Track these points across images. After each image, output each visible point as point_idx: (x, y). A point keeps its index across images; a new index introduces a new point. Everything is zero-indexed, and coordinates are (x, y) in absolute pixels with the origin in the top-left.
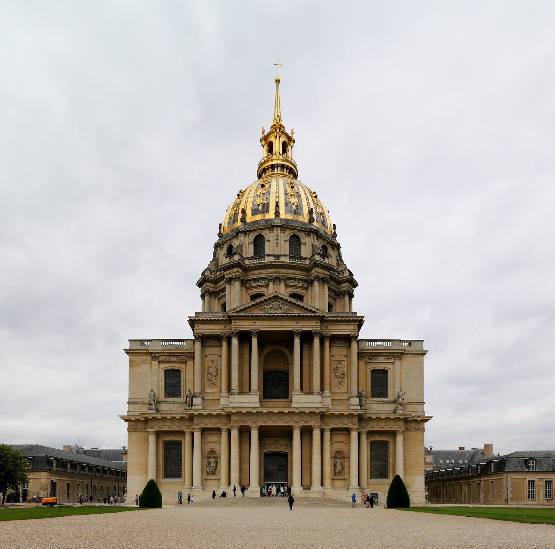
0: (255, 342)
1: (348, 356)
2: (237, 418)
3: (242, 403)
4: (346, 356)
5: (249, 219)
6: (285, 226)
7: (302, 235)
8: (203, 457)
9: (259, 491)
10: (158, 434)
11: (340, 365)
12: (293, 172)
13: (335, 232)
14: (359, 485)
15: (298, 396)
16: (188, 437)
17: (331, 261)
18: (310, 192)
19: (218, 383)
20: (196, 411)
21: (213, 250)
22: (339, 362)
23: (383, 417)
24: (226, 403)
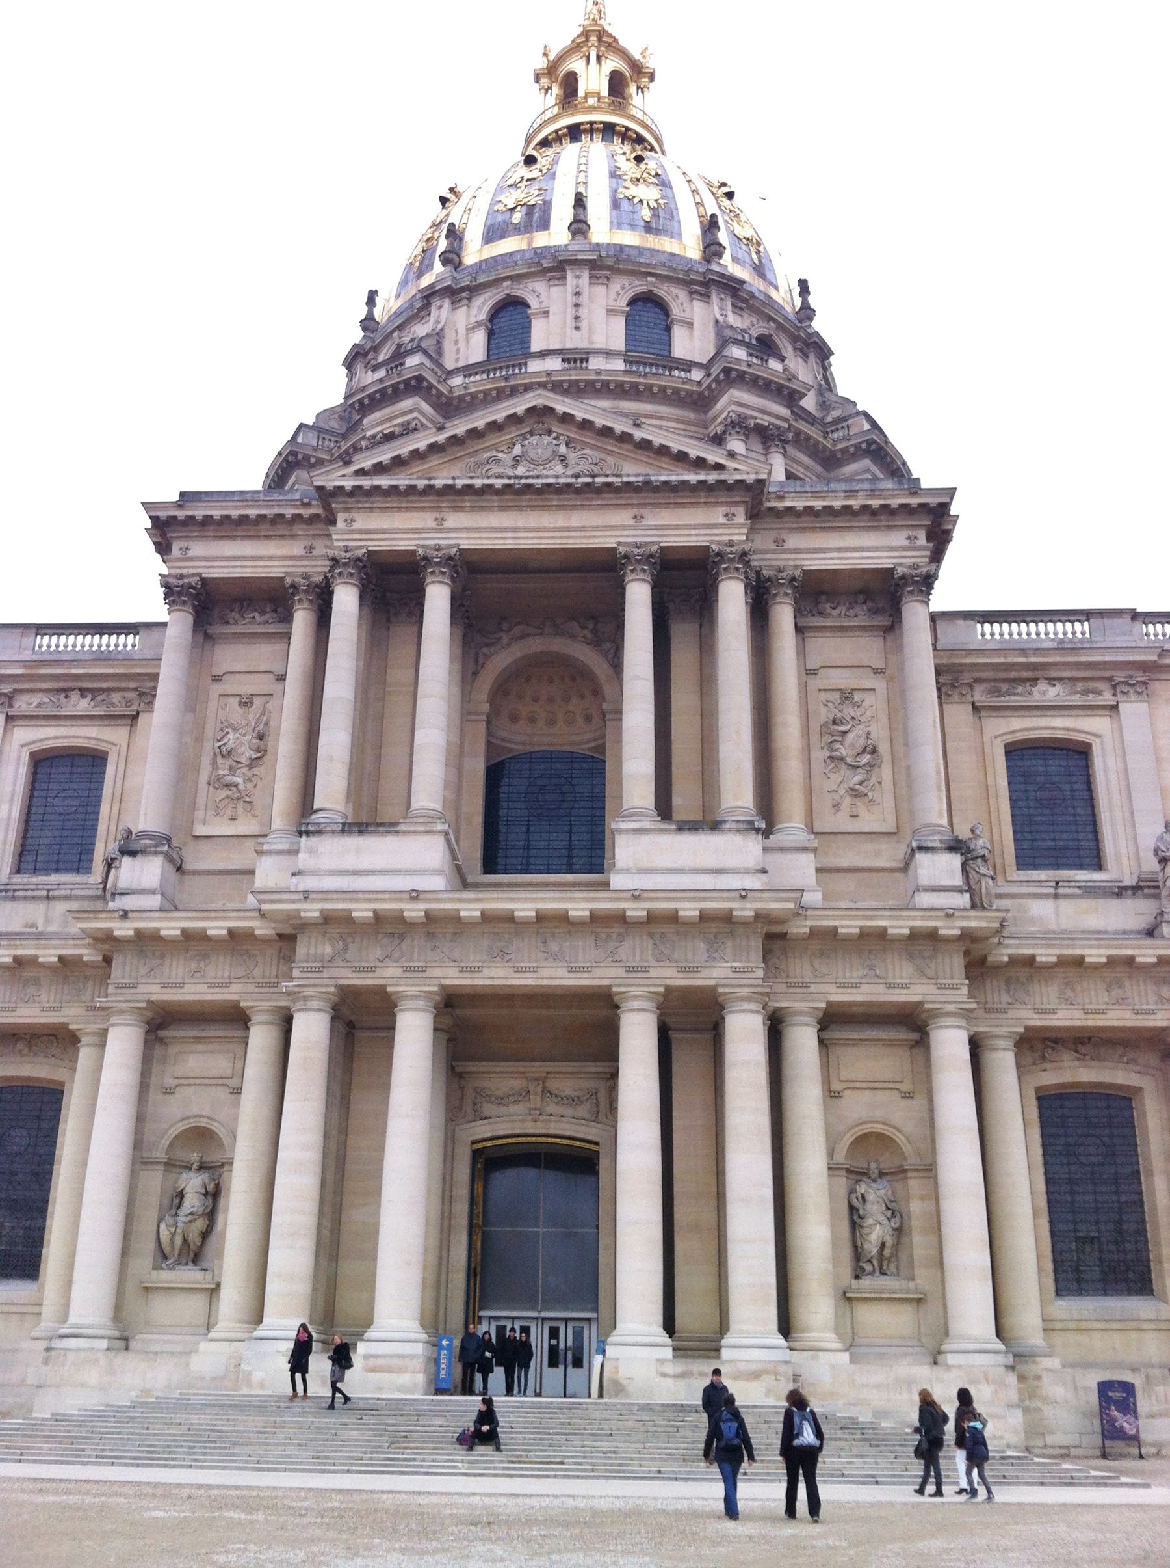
1: (892, 672)
2: (328, 950)
3: (356, 873)
7: (679, 301)
9: (419, 1364)
14: (999, 1333)
15: (646, 839)
18: (709, 185)
20: (125, 915)
23: (1095, 954)
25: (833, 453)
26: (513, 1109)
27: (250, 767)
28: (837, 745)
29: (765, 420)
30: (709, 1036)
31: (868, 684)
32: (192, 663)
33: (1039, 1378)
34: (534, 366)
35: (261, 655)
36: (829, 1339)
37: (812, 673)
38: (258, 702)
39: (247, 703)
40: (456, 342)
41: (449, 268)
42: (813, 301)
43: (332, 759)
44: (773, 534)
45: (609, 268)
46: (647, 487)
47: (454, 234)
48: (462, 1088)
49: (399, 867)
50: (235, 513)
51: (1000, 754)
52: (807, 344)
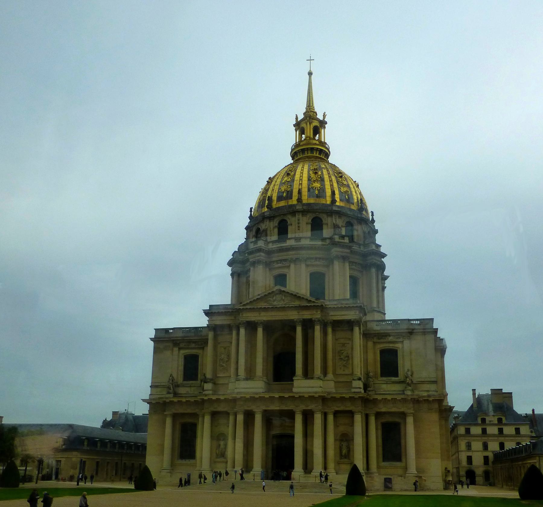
5: (275, 205)
6: (308, 209)
7: (324, 217)
15: (299, 381)
23: (389, 397)
29: (344, 254)
31: (348, 342)
36: (333, 471)
37: (336, 340)
46: (300, 306)
47: (270, 199)
51: (378, 352)
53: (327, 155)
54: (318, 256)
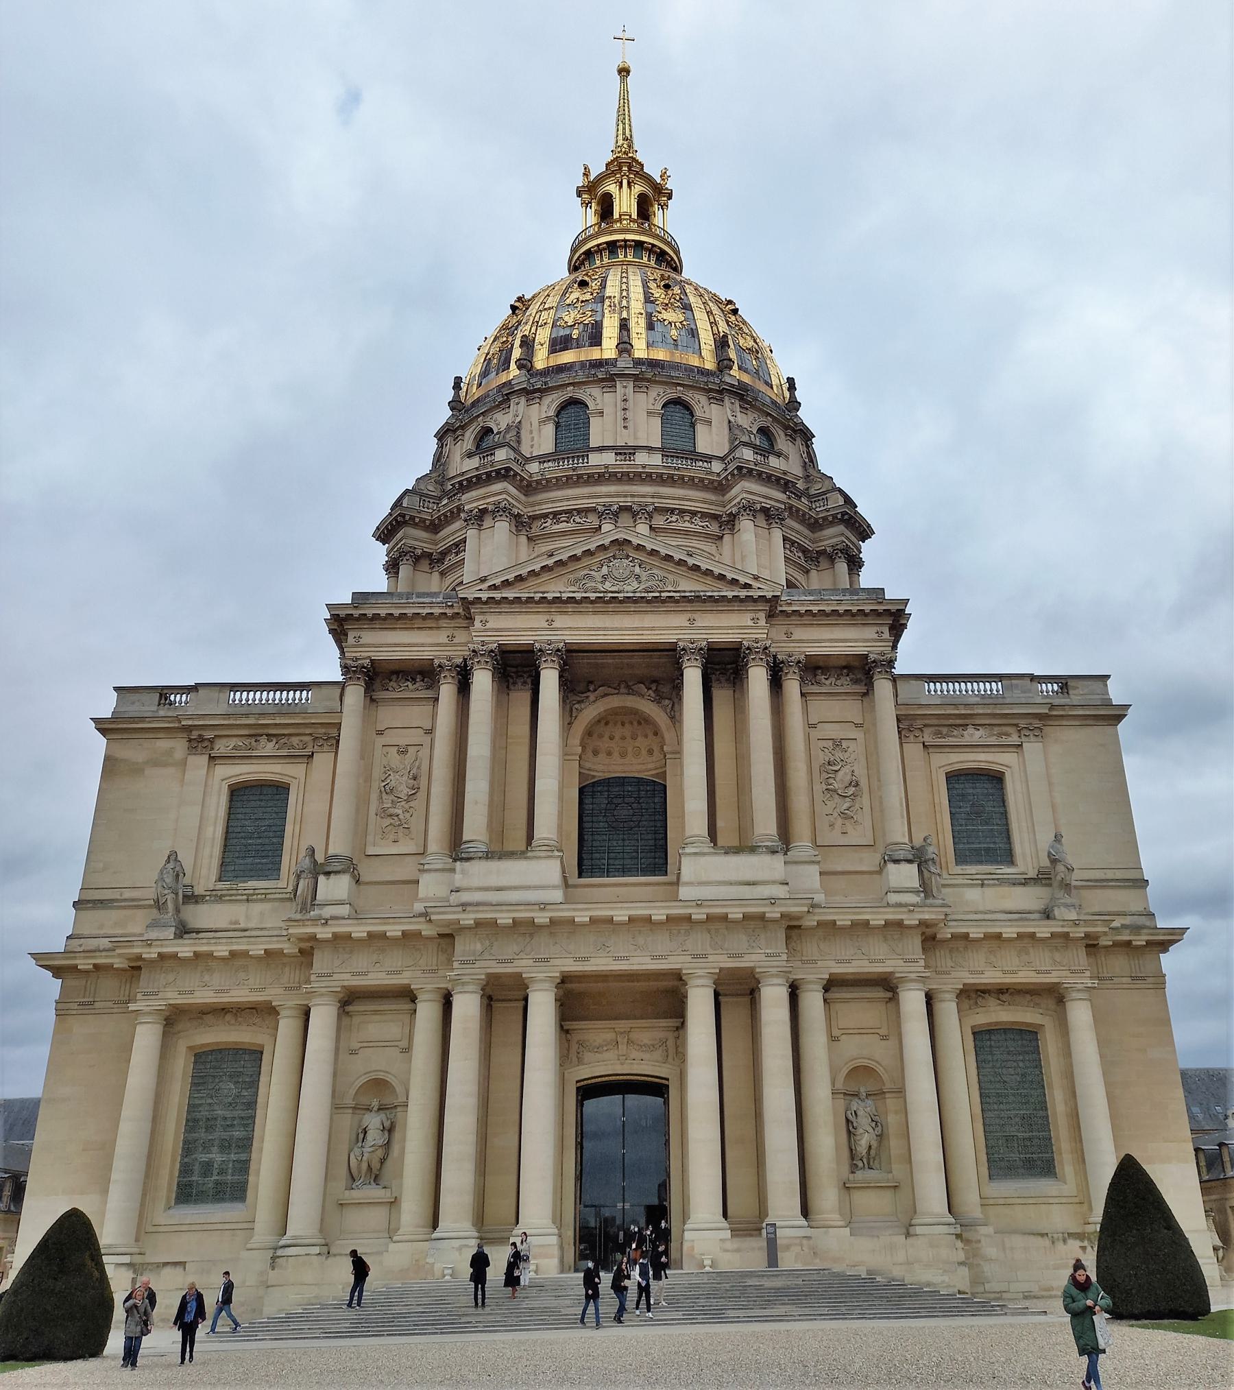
0: (550, 679)
2: (479, 947)
4: (857, 726)
5: (541, 360)
6: (648, 373)
8: (336, 1107)
9: (556, 1251)
10: (173, 1019)
11: (839, 755)
12: (666, 259)
13: (792, 396)
15: (703, 860)
16: (287, 1027)
17: (788, 463)
18: (717, 301)
19: (416, 824)
21: (433, 444)
22: (837, 743)
24: (443, 892)
25: (816, 520)
26: (606, 1055)
27: (407, 801)
28: (831, 781)
29: (768, 504)
30: (747, 999)
32: (364, 721)
33: (979, 1241)
34: (595, 459)
35: (416, 714)
37: (812, 726)
38: (412, 750)
39: (403, 751)
40: (531, 432)
41: (524, 371)
42: (798, 395)
43: (476, 803)
44: (784, 629)
45: (648, 380)
46: (698, 599)
47: (528, 344)
48: (568, 1041)
49: (528, 884)
50: (396, 612)
52: (795, 431)
53: (677, 269)
54: (688, 505)
